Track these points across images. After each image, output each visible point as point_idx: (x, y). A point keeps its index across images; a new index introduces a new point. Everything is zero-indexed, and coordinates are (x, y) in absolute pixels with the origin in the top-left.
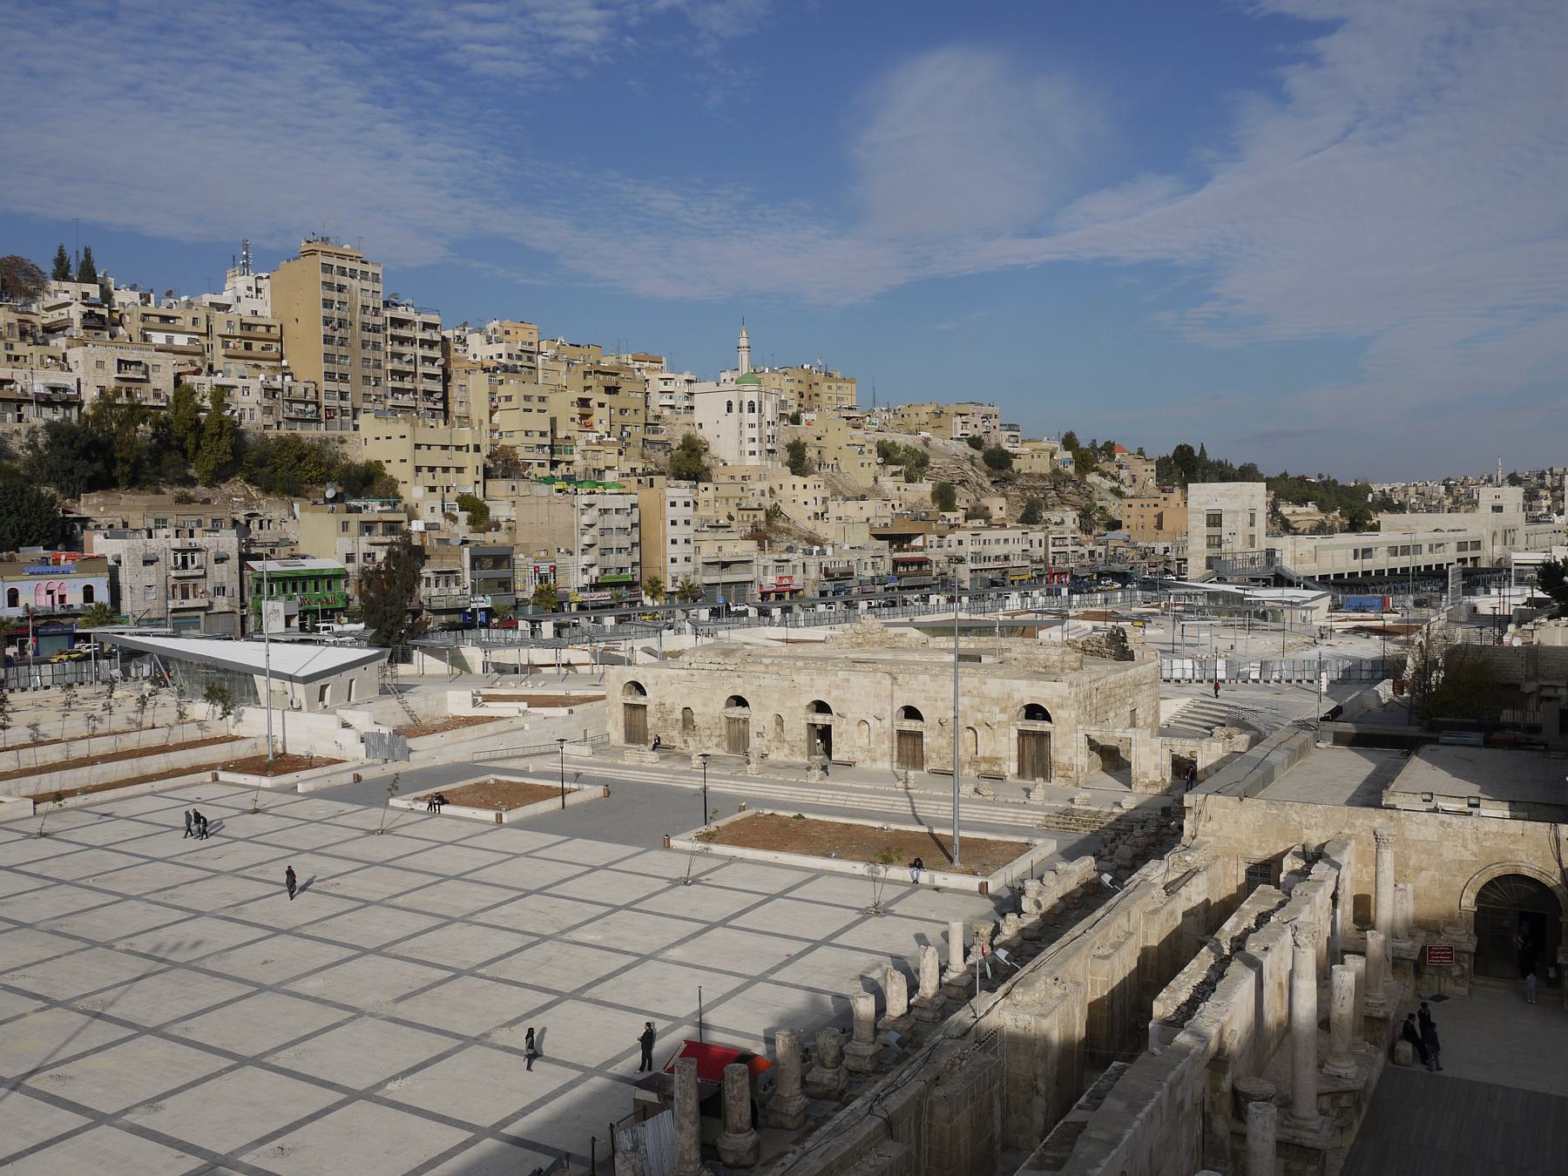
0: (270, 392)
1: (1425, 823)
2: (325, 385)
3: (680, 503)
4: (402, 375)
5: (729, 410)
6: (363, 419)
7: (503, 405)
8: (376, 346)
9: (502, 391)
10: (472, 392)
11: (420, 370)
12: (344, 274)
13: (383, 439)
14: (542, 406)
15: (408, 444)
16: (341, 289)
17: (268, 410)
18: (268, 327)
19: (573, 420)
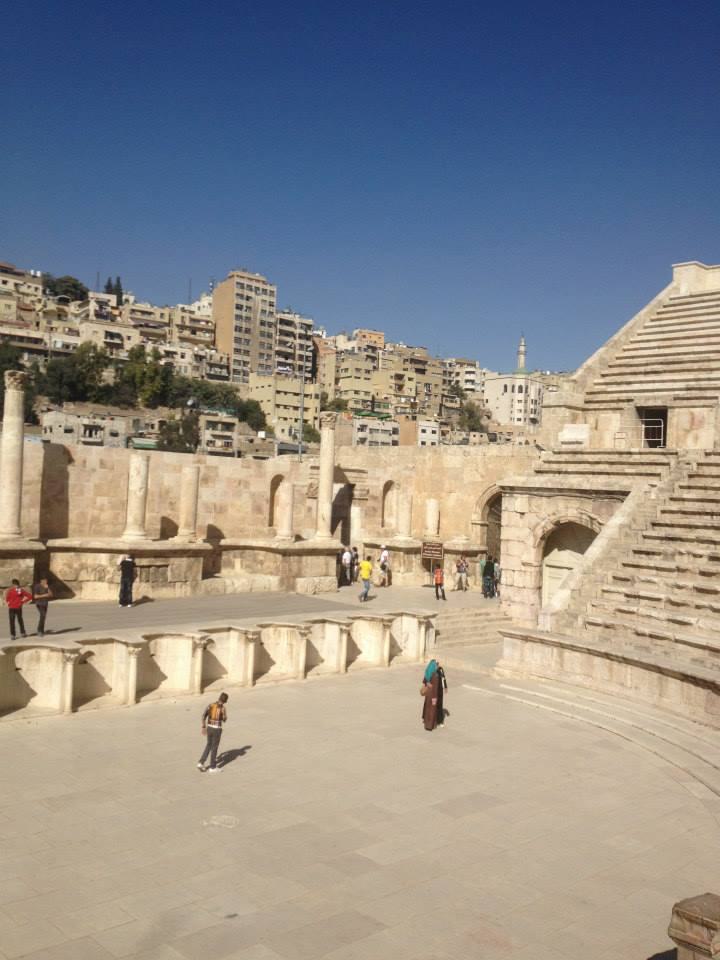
0: (199, 358)
1: (454, 454)
2: (234, 357)
3: (429, 431)
4: (287, 356)
5: (506, 390)
6: (252, 377)
7: (343, 374)
8: (270, 336)
9: (344, 366)
10: (327, 366)
11: (298, 352)
12: (251, 290)
13: (266, 387)
14: (368, 376)
15: (272, 390)
16: (248, 298)
17: (196, 368)
18: (207, 322)
19: (391, 387)
